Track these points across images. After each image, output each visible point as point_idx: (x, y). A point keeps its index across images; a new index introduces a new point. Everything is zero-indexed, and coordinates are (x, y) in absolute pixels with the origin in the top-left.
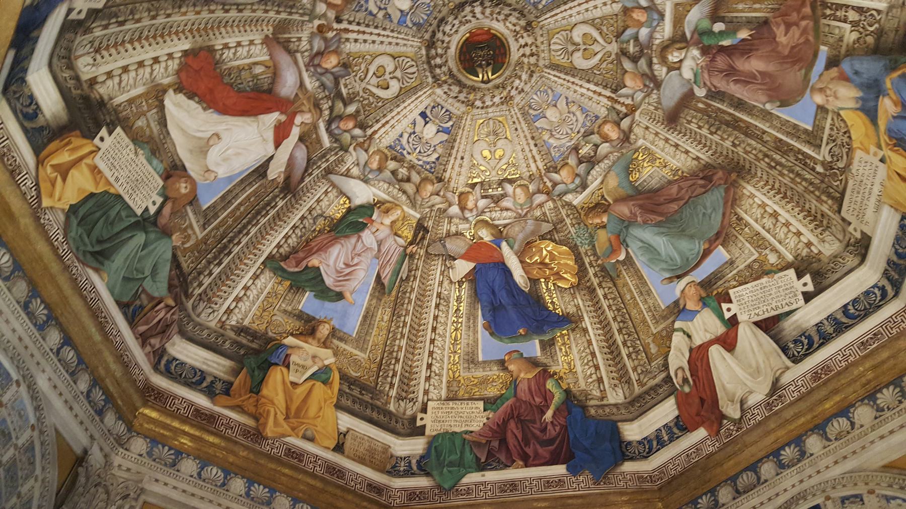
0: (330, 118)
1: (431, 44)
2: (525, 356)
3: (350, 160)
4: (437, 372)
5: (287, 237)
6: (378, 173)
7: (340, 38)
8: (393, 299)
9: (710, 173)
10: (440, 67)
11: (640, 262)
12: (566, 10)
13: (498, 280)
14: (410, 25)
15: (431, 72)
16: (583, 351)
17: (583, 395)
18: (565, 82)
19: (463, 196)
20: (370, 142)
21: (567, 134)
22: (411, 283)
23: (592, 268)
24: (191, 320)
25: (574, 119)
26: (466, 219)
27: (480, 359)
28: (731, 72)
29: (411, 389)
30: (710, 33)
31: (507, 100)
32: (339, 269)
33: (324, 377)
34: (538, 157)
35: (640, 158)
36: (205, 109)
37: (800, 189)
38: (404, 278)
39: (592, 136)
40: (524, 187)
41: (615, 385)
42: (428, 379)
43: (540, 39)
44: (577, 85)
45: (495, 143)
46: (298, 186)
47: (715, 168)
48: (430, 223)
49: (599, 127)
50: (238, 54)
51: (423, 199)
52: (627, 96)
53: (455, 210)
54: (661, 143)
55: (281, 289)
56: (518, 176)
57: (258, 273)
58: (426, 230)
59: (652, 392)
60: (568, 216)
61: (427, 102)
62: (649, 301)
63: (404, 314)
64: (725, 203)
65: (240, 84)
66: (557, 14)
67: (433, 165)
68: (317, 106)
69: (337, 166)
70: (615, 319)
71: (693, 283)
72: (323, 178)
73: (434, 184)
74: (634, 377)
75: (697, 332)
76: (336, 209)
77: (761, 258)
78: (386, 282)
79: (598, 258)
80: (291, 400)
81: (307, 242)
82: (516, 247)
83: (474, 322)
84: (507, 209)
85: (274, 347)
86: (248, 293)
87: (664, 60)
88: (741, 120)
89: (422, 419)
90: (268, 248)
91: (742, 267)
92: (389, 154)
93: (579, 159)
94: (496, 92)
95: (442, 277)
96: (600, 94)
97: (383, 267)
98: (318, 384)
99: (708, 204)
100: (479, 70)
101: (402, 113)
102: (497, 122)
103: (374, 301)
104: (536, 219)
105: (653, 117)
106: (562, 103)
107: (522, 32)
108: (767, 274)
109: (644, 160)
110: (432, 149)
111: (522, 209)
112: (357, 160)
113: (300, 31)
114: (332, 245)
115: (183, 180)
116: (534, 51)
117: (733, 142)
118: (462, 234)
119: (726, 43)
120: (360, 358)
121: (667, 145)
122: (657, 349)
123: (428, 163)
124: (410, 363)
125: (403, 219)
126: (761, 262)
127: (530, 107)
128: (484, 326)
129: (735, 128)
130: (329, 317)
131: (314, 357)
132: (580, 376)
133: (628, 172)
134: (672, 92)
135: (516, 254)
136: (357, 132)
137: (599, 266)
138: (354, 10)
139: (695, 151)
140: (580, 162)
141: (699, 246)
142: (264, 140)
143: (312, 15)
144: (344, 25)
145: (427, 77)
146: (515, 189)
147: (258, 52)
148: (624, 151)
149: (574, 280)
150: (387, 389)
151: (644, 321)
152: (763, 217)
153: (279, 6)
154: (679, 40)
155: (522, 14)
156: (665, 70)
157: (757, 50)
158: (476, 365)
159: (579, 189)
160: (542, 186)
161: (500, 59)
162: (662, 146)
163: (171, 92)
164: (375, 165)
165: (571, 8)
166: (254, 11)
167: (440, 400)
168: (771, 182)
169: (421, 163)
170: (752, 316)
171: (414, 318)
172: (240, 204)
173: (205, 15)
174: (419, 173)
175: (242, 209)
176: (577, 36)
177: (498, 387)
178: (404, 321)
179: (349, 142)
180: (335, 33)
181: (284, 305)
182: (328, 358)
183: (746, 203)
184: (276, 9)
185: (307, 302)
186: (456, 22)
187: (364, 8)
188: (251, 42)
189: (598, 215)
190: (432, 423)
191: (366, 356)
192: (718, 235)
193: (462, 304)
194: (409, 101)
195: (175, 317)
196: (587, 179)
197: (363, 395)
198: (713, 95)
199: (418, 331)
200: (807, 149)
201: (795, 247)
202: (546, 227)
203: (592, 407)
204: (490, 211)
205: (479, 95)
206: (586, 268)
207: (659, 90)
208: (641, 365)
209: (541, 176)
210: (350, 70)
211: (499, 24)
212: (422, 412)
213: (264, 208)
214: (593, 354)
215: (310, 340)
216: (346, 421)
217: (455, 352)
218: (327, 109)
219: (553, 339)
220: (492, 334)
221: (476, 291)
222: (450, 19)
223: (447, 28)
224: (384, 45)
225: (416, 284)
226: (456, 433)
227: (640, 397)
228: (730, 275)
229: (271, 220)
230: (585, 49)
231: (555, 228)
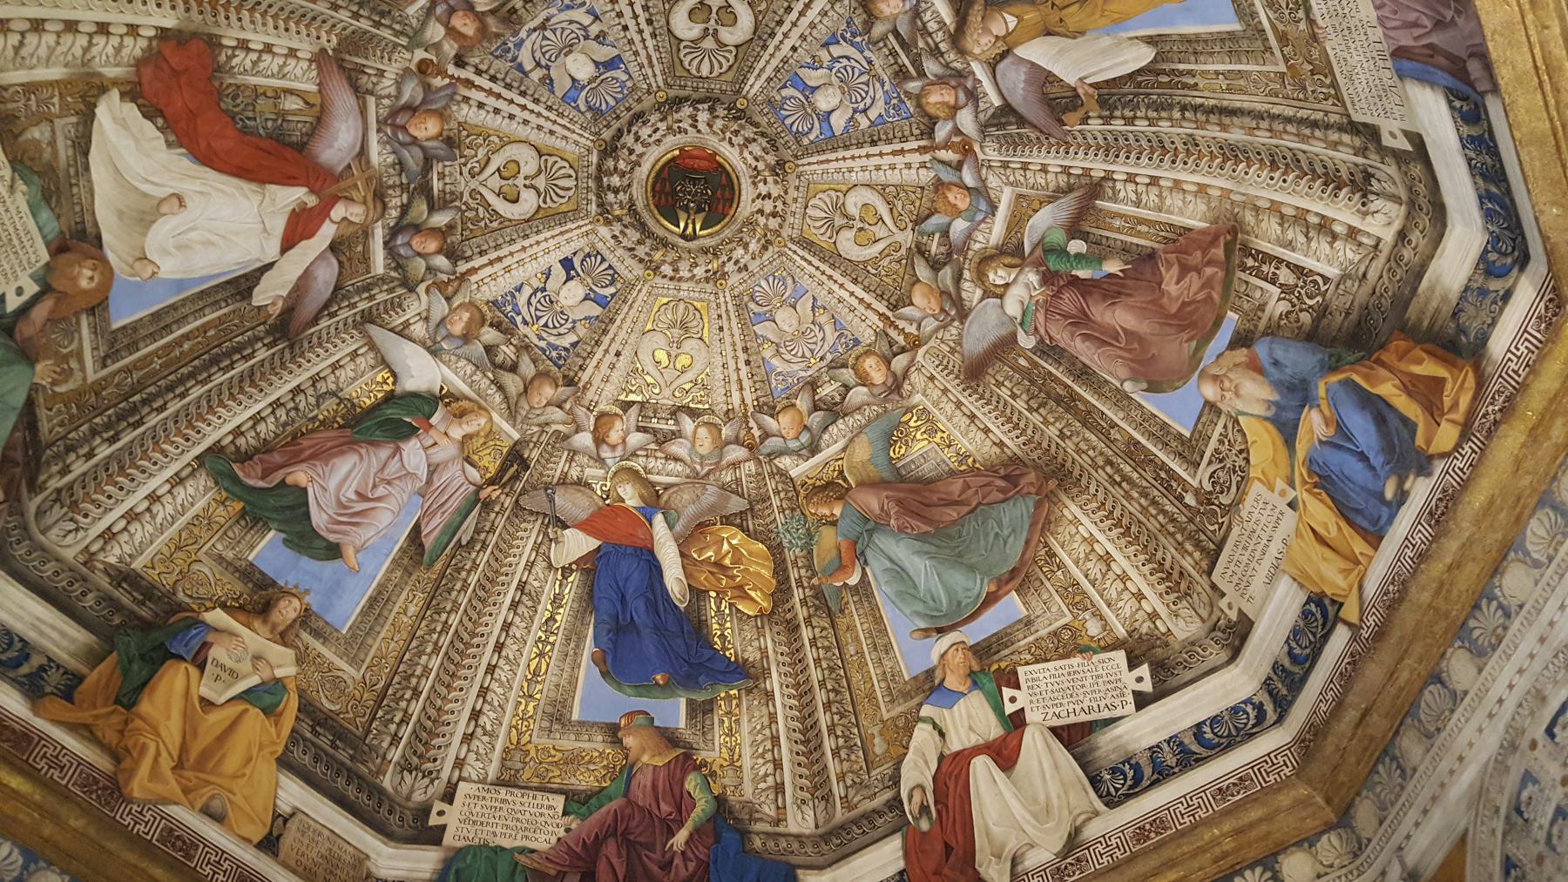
0: (397, 224)
1: (610, 150)
2: (657, 723)
3: (414, 307)
4: (489, 728)
5: (257, 419)
6: (460, 343)
7: (455, 93)
8: (434, 577)
9: (1018, 472)
10: (616, 191)
11: (882, 593)
12: (844, 159)
13: (636, 578)
14: (583, 108)
15: (599, 196)
16: (759, 732)
17: (747, 810)
18: (818, 273)
19: (604, 420)
20: (460, 285)
21: (803, 356)
22: (474, 555)
23: (800, 590)
25: (820, 336)
26: (601, 461)
27: (575, 717)
28: (1080, 321)
29: (432, 752)
30: (1062, 252)
31: (717, 277)
32: (343, 500)
33: (268, 699)
34: (747, 383)
35: (912, 424)
36: (169, 145)
37: (1153, 525)
38: (464, 542)
39: (843, 370)
40: (714, 430)
41: (803, 802)
42: (468, 738)
43: (793, 193)
44: (836, 281)
45: (679, 345)
46: (304, 330)
47: (1025, 465)
48: (535, 454)
49: (857, 358)
50: (262, 65)
51: (532, 408)
52: (910, 321)
53: (584, 440)
54: (949, 408)
55: (220, 514)
56: (707, 406)
57: (184, 474)
58: (525, 465)
59: (865, 822)
60: (777, 492)
61: (582, 242)
62: (885, 662)
63: (448, 609)
64: (1033, 525)
65: (249, 119)
66: (828, 161)
67: (563, 353)
68: (380, 197)
69: (386, 312)
70: (822, 684)
71: (961, 646)
72: (355, 327)
73: (557, 386)
74: (838, 790)
75: (957, 731)
76: (364, 387)
77: (1076, 625)
78: (428, 543)
79: (814, 574)
81: (294, 437)
83: (577, 646)
84: (677, 459)
85: (182, 623)
86: (156, 508)
87: (980, 277)
88: (1082, 399)
89: (441, 813)
90: (216, 431)
91: (1043, 632)
92: (489, 315)
93: (814, 401)
94: (701, 260)
95: (534, 554)
96: (869, 306)
97: (428, 514)
98: (255, 713)
99: (1006, 521)
100: (682, 216)
101: (530, 252)
102: (691, 308)
103: (399, 574)
104: (723, 487)
105: (945, 363)
106: (805, 305)
107: (766, 173)
108: (1081, 652)
109: (917, 428)
110: (569, 325)
111: (701, 465)
112: (428, 310)
113: (386, 60)
114: (343, 453)
115: (91, 262)
116: (778, 209)
117: (1061, 431)
118: (588, 485)
119: (1083, 273)
120: (345, 677)
121: (958, 412)
122: (885, 746)
123: (556, 348)
124: (439, 702)
125: (487, 436)
127: (752, 298)
128: (593, 657)
130: (302, 588)
131: (257, 658)
132: (747, 775)
133: (889, 441)
134: (981, 331)
135: (676, 540)
136: (441, 261)
137: (812, 587)
138: (492, 54)
139: (998, 433)
140: (816, 408)
141: (981, 586)
142: (265, 230)
143: (415, 39)
145: (589, 202)
146: (696, 427)
147: (299, 72)
148: (889, 406)
150: (385, 745)
151: (871, 696)
152: (1087, 559)
153: (361, 5)
154: (1011, 252)
155: (773, 144)
156: (979, 293)
157: (1130, 295)
158: (564, 725)
159: (804, 452)
160: (743, 433)
161: (720, 206)
162: (949, 413)
164: (458, 328)
165: (853, 158)
167: (483, 781)
168: (1108, 505)
169: (542, 344)
170: (1049, 717)
171: (465, 620)
172: (186, 337)
174: (534, 361)
175: (186, 346)
176: (853, 203)
177: (596, 773)
178: (446, 622)
179: (421, 276)
180: (447, 81)
181: (220, 547)
182: (282, 662)
183: (1065, 531)
184: (355, 8)
186: (662, 126)
187: (510, 56)
188: (292, 53)
189: (827, 502)
191: (359, 676)
192: (1014, 572)
193: (561, 610)
194: (548, 234)
196: (821, 437)
197: (336, 748)
198: (1046, 349)
199: (468, 645)
200: (1176, 466)
201: (1131, 616)
202: (736, 504)
203: (757, 834)
204: (647, 456)
205: (671, 256)
207: (962, 323)
208: (853, 772)
209: (745, 416)
210: (457, 152)
211: (731, 149)
212: (442, 800)
213: (228, 354)
214: (775, 740)
215: (257, 624)
216: (293, 793)
217: (531, 696)
218: (395, 208)
219: (711, 702)
220: (604, 674)
221: (591, 591)
222: (654, 118)
223: (645, 132)
224: (528, 129)
226: (503, 849)
227: (842, 827)
228: (1022, 643)
229: (235, 381)
230: (861, 229)
231: (752, 509)
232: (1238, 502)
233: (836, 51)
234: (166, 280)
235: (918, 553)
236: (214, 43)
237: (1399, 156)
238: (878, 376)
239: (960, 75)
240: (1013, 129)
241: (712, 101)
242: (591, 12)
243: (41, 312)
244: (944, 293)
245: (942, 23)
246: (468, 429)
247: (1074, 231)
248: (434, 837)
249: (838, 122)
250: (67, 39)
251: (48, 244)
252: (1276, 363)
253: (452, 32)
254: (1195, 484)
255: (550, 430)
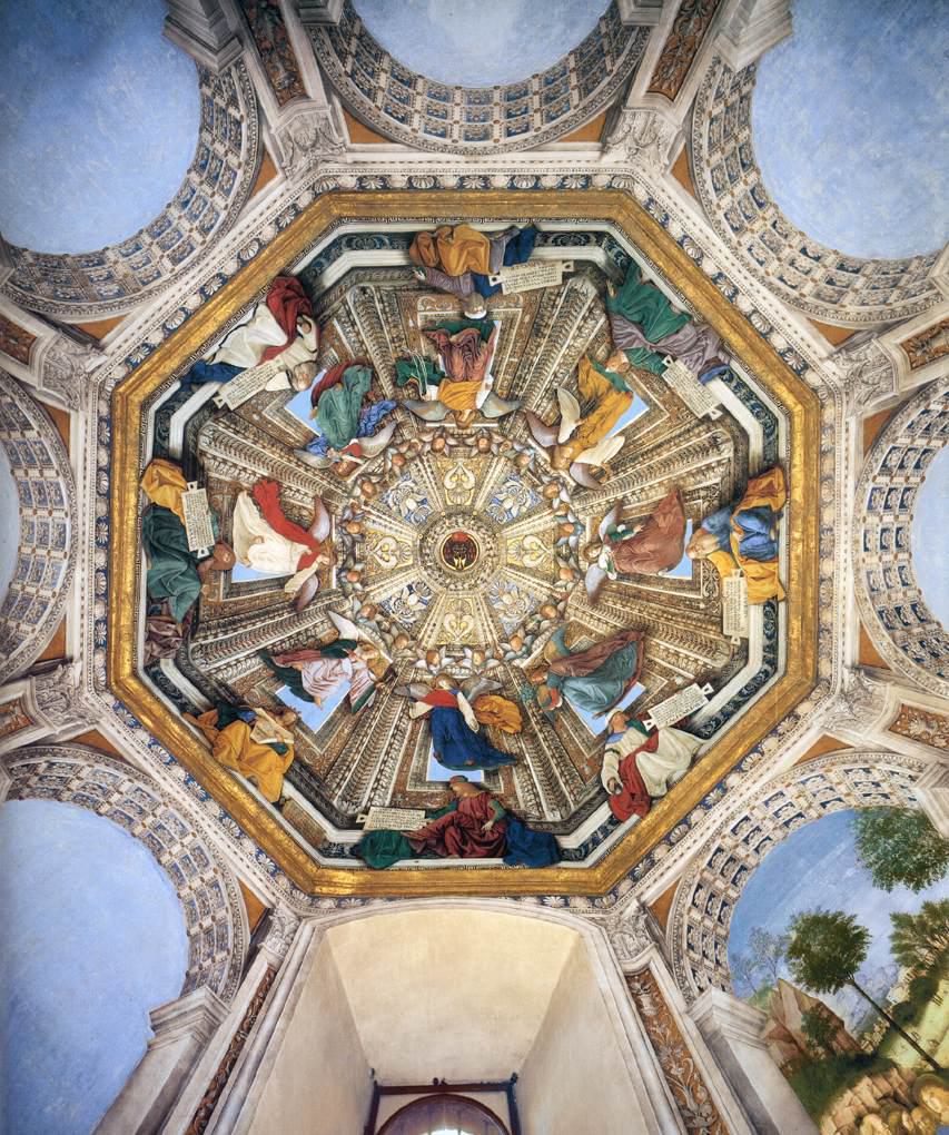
2: (470, 780)
3: (347, 605)
5: (283, 641)
11: (575, 706)
13: (451, 719)
24: (187, 658)
27: (427, 779)
28: (632, 557)
30: (616, 533)
34: (494, 631)
42: (374, 789)
45: (461, 618)
48: (400, 670)
52: (561, 587)
53: (422, 663)
54: (588, 618)
58: (396, 675)
60: (515, 677)
70: (553, 756)
74: (570, 799)
78: (353, 703)
80: (247, 751)
82: (469, 698)
84: (466, 668)
87: (586, 556)
90: (266, 643)
91: (656, 692)
96: (542, 586)
97: (353, 691)
104: (489, 678)
119: (627, 537)
126: (672, 683)
129: (639, 598)
130: (297, 710)
131: (276, 732)
132: (521, 800)
134: (592, 581)
135: (469, 702)
136: (358, 586)
139: (613, 622)
141: (621, 685)
144: (368, 509)
149: (519, 729)
151: (579, 752)
154: (596, 542)
163: (245, 492)
164: (365, 614)
166: (315, 475)
167: (383, 806)
172: (258, 597)
173: (284, 461)
176: (527, 543)
185: (284, 692)
189: (540, 675)
190: (370, 823)
192: (635, 675)
195: (178, 646)
202: (496, 685)
206: (529, 719)
213: (274, 611)
214: (533, 785)
215: (277, 718)
220: (440, 762)
223: (438, 529)
225: (378, 715)
227: (576, 813)
232: (720, 595)
233: (508, 484)
234: (255, 572)
235: (589, 682)
236: (279, 485)
237: (720, 420)
238: (553, 614)
239: (557, 478)
240: (583, 494)
241: (464, 513)
242: (414, 482)
243: (209, 563)
244: (573, 570)
245: (545, 460)
246: (372, 656)
247: (618, 523)
248: (361, 827)
249: (514, 512)
250: (233, 469)
251: (215, 538)
252: (712, 527)
253: (363, 491)
254: (701, 597)
255: (406, 660)
